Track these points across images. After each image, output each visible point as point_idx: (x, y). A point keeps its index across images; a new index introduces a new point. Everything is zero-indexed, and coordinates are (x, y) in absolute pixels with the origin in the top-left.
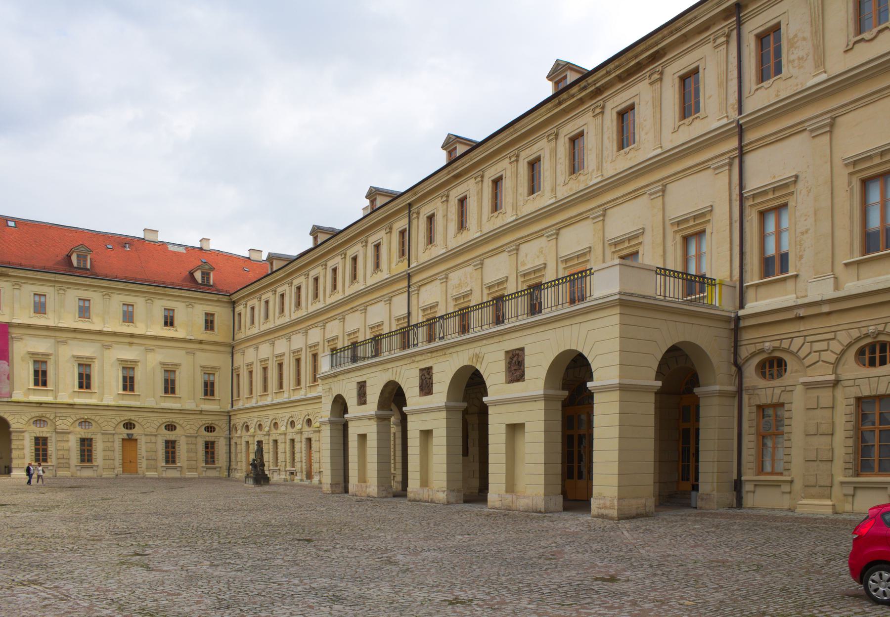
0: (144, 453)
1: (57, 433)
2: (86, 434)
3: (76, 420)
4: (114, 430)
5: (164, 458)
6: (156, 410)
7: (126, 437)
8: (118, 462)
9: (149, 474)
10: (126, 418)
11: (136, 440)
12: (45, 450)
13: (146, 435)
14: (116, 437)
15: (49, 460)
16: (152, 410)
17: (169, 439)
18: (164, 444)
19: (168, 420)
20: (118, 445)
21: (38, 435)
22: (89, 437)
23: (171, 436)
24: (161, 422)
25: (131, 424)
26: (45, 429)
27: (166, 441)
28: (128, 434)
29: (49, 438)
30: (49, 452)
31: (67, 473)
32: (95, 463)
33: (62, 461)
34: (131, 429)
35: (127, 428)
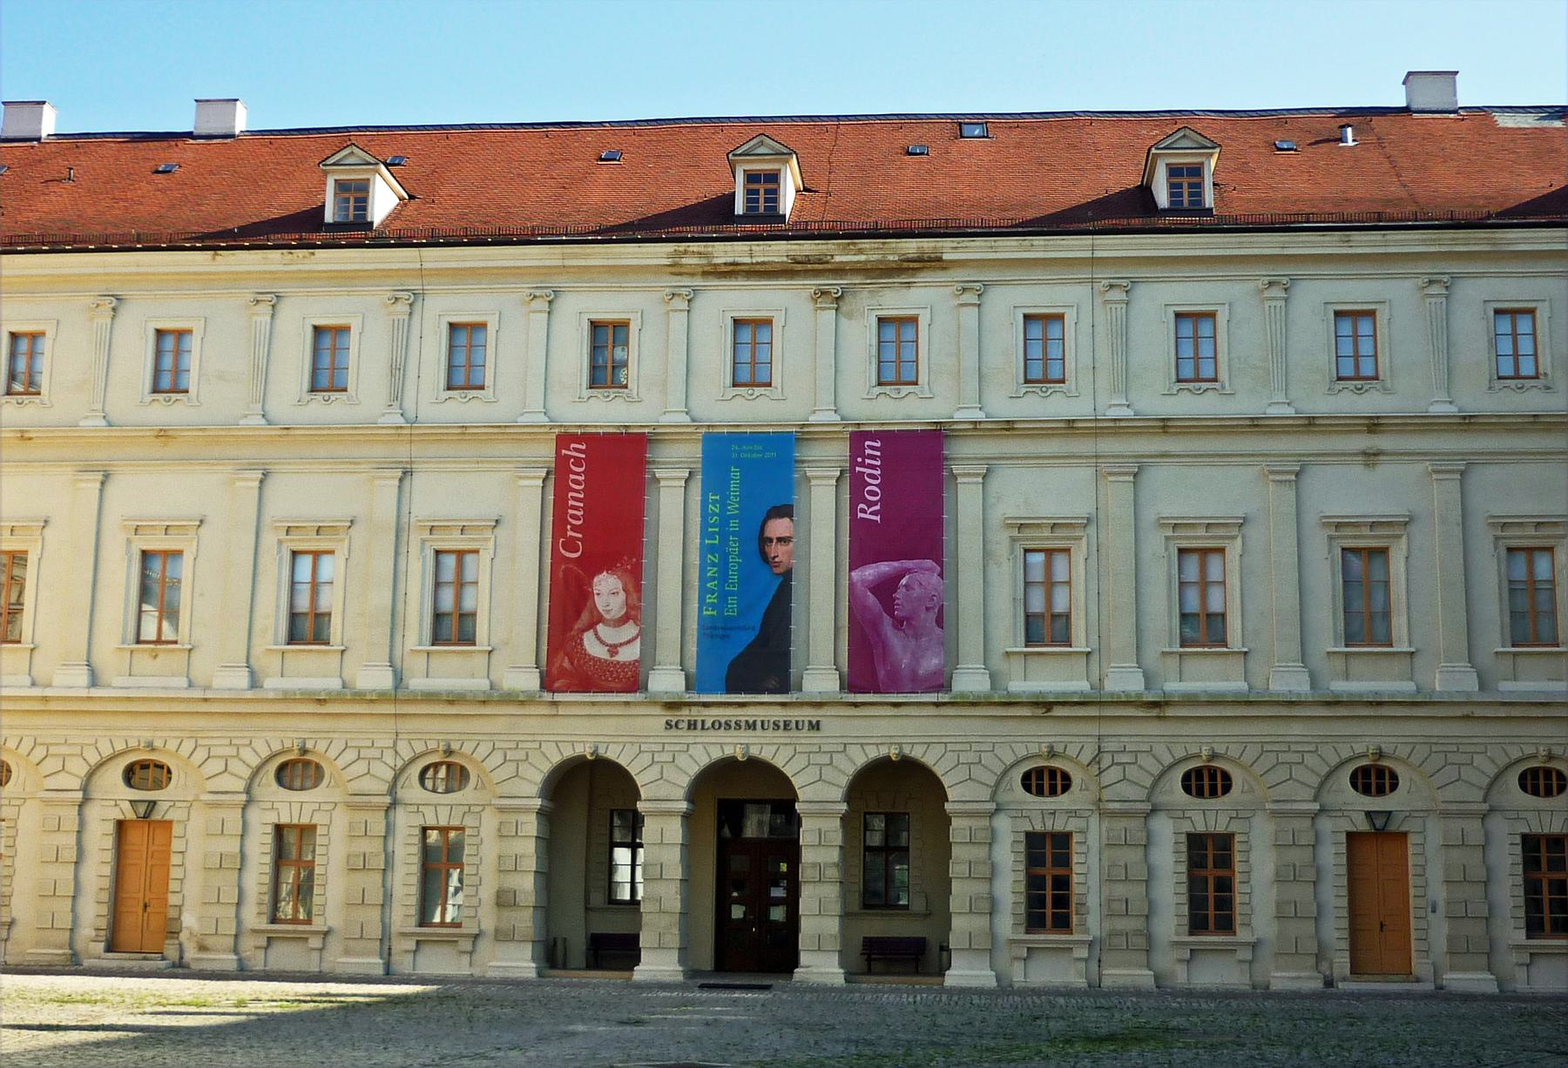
0: (1438, 892)
1: (1103, 814)
2: (1211, 817)
3: (1171, 766)
4: (1315, 800)
5: (1522, 913)
6: (1479, 712)
7: (1363, 826)
8: (1335, 930)
9: (1464, 979)
10: (1359, 748)
11: (1405, 835)
12: (1063, 883)
13: (1446, 814)
14: (1325, 824)
15: (1075, 919)
16: (1465, 711)
17: (1536, 829)
18: (1518, 850)
19: (1530, 750)
20: (1333, 856)
21: (1039, 828)
22: (1221, 829)
23: (1546, 818)
24: (1503, 761)
25: (1381, 772)
26: (1063, 801)
27: (1525, 837)
28: (1369, 814)
29: (1076, 838)
30: (1076, 889)
31: (1142, 977)
32: (1242, 935)
33: (1121, 924)
34: (1381, 791)
35: (1366, 791)
